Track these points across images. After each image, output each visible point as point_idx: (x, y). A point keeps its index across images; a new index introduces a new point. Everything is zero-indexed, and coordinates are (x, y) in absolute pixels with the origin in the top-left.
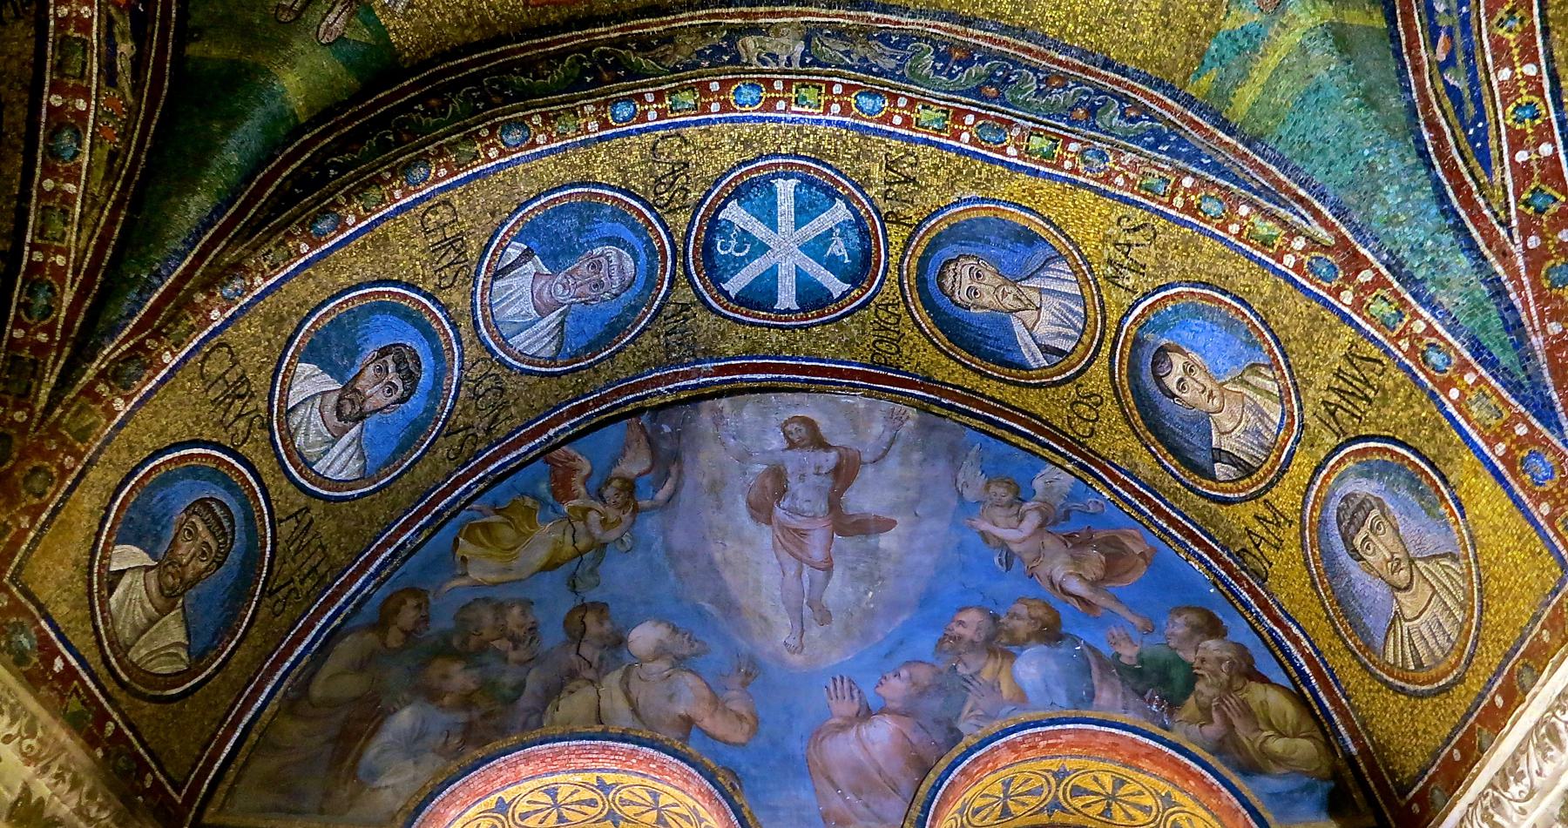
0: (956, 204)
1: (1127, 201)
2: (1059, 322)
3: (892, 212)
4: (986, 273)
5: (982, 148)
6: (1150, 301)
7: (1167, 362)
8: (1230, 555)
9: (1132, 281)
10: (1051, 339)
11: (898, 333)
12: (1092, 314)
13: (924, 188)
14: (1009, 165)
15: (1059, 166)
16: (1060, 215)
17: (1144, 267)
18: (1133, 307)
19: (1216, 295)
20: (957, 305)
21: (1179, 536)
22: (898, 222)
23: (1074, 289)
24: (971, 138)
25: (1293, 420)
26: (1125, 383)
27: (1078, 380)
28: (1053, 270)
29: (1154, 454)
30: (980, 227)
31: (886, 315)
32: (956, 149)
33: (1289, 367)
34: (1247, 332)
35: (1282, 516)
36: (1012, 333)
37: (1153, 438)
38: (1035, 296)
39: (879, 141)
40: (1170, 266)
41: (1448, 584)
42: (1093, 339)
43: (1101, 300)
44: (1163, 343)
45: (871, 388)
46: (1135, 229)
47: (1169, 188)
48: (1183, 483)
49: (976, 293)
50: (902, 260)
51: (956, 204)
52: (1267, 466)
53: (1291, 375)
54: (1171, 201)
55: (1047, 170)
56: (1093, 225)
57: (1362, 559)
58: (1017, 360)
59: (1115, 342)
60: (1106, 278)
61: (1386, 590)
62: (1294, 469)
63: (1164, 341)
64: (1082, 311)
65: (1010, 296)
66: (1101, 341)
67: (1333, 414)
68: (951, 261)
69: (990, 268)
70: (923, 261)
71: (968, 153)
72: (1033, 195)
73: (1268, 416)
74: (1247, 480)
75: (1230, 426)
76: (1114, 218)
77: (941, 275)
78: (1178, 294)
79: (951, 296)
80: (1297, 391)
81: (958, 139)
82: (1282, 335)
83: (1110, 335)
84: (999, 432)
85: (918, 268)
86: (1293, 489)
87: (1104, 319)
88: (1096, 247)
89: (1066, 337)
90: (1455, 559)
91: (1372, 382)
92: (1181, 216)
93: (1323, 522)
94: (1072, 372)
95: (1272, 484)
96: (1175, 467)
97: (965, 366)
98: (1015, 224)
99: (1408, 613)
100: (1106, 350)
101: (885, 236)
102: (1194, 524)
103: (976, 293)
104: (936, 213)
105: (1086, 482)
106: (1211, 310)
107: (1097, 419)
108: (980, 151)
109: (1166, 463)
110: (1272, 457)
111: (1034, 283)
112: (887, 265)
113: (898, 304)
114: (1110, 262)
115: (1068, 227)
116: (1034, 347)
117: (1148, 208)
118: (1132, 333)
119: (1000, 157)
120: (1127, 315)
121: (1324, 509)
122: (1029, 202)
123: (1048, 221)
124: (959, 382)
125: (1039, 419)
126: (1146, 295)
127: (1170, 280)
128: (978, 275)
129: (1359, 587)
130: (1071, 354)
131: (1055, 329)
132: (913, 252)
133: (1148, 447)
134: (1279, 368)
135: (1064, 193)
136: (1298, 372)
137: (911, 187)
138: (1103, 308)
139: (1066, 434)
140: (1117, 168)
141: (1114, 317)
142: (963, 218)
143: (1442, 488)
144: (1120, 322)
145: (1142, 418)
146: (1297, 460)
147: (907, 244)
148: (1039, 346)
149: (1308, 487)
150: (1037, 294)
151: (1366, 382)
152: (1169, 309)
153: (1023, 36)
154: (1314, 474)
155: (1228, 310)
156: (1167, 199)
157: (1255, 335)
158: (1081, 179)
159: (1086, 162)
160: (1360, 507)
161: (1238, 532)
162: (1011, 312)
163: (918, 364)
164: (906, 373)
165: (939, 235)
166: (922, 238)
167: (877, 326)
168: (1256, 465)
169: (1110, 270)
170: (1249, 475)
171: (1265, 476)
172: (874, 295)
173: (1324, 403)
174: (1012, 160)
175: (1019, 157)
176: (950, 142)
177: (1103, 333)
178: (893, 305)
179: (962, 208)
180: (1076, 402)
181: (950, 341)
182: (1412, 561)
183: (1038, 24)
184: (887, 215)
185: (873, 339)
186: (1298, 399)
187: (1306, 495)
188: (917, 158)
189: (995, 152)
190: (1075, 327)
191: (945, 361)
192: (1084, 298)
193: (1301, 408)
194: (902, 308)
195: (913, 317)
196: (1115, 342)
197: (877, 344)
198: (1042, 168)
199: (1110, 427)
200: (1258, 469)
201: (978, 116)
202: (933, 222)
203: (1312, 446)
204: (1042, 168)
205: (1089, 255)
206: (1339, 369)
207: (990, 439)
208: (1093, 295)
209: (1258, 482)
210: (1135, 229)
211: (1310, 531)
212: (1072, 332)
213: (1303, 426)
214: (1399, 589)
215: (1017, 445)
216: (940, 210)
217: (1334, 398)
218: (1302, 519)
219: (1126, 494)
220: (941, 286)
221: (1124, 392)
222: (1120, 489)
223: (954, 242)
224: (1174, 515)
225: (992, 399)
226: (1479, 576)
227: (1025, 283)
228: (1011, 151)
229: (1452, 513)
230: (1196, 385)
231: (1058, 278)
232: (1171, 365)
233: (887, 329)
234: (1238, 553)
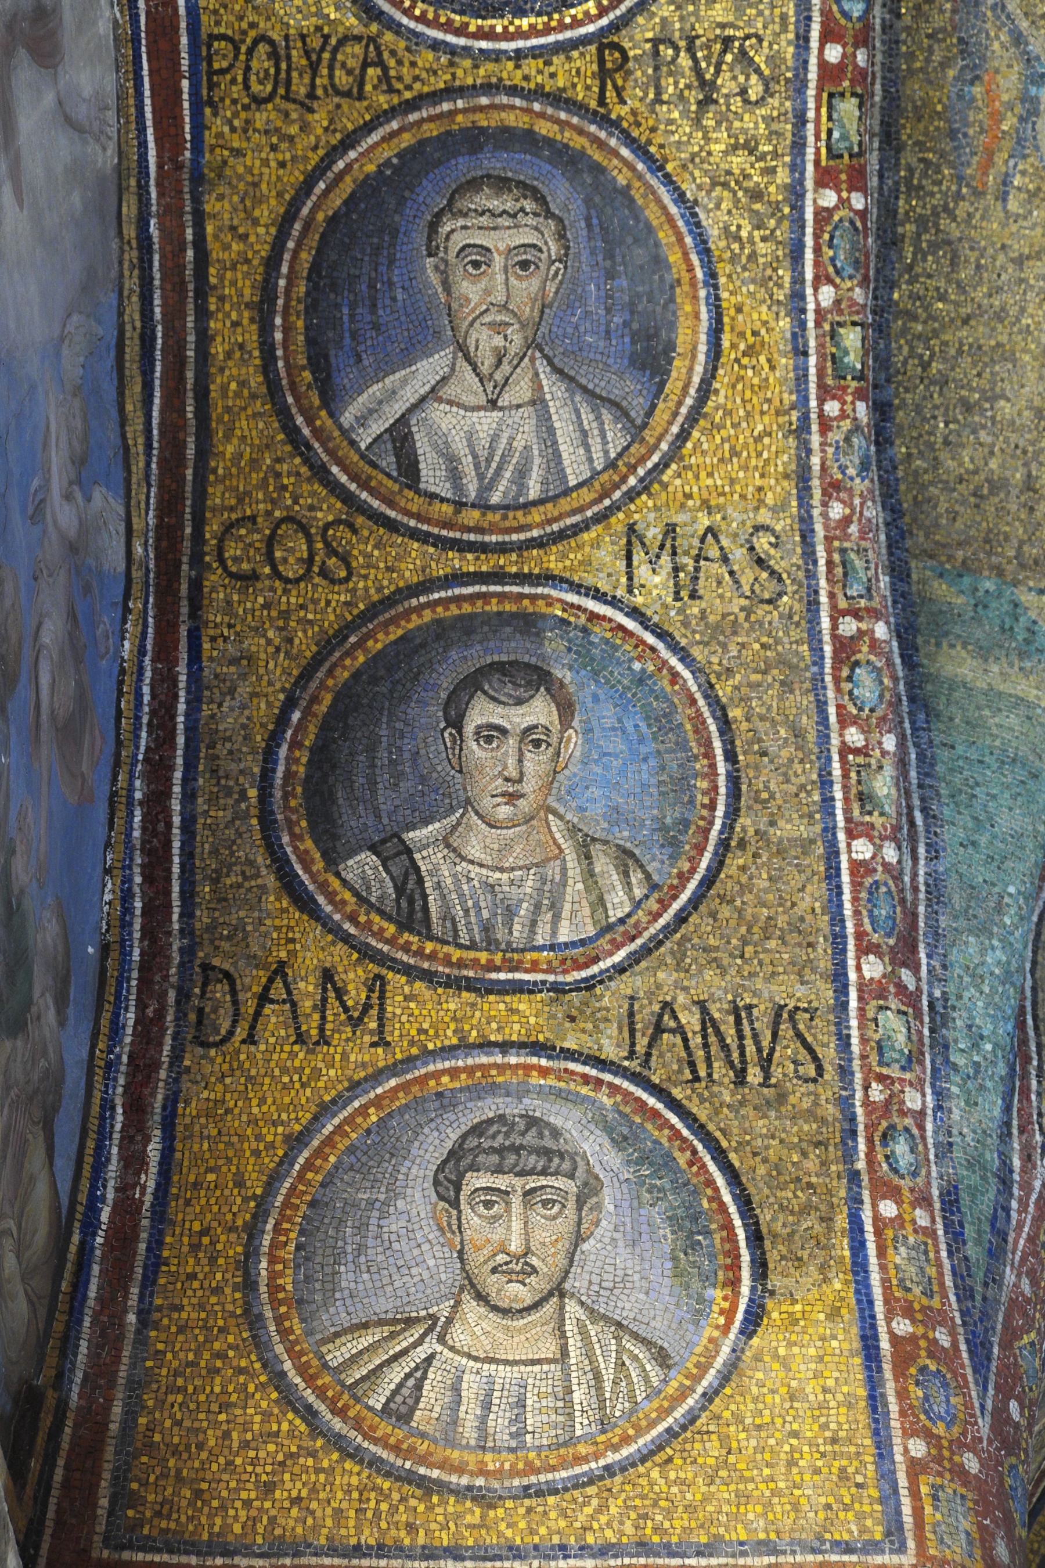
0: (680, 198)
1: (807, 536)
2: (483, 454)
3: (623, 52)
4: (535, 283)
5: (817, 236)
6: (631, 624)
7: (520, 692)
8: (188, 952)
9: (657, 579)
10: (435, 446)
11: (312, 95)
12: (536, 516)
13: (697, 122)
14: (797, 295)
15: (825, 393)
16: (728, 413)
17: (694, 595)
18: (598, 595)
19: (717, 745)
20: (433, 227)
21: (136, 834)
22: (603, 74)
23: (575, 471)
24: (829, 211)
25: (586, 966)
26: (415, 621)
27: (360, 520)
28: (598, 418)
29: (282, 720)
30: (640, 256)
31: (351, 63)
32: (801, 181)
33: (681, 919)
34: (686, 823)
35: (381, 1019)
36: (409, 355)
37: (323, 708)
38: (520, 391)
39: (784, 17)
40: (724, 646)
41: (608, 1376)
42: (479, 530)
43: (577, 530)
44: (558, 673)
45: (136, 40)
46: (760, 562)
47: (863, 603)
48: (264, 797)
49: (476, 264)
50: (514, 91)
51: (680, 198)
52: (456, 954)
53: (669, 930)
54: (844, 613)
55: (812, 371)
56: (732, 482)
57: (455, 1204)
58: (345, 378)
59: (498, 576)
60: (631, 529)
61: (450, 1275)
62: (496, 1005)
63: (561, 673)
64: (534, 492)
65: (498, 341)
66: (483, 548)
67: (659, 1029)
68: (541, 199)
69: (551, 288)
70: (529, 140)
71: (798, 208)
72: (750, 351)
73: (557, 918)
74: (391, 929)
75: (474, 851)
76: (764, 517)
77: (502, 184)
78: (675, 676)
79: (450, 208)
80: (646, 951)
81: (820, 183)
82: (725, 884)
83: (510, 563)
84: (132, 368)
85: (505, 130)
86: (454, 1019)
87: (539, 543)
88: (689, 496)
89: (455, 476)
90: (662, 1358)
91: (777, 1073)
92: (827, 638)
93: (445, 1101)
94: (376, 504)
95: (428, 977)
96: (289, 775)
97: (272, 263)
98: (672, 326)
99: (459, 1336)
100: (469, 563)
101: (563, 48)
102: (188, 854)
103: (476, 264)
104: (641, 150)
105: (127, 596)
106: (682, 745)
107: (287, 581)
108: (809, 230)
109: (283, 752)
110: (483, 957)
111: (553, 388)
112: (497, 56)
113: (391, 90)
114: (671, 530)
115: (709, 433)
116: (397, 409)
117: (811, 575)
118: (541, 606)
119: (809, 275)
120: (577, 588)
121: (477, 1092)
122: (734, 346)
123: (705, 391)
124: (216, 252)
125: (203, 453)
126: (635, 613)
127: (696, 652)
128: (524, 265)
129: (394, 1225)
130: (418, 492)
131: (460, 446)
132: (542, 115)
133: (290, 703)
134: (664, 906)
135: (778, 413)
136: (685, 939)
137: (694, 96)
138: (561, 536)
139: (199, 523)
140: (857, 501)
141: (553, 563)
142: (652, 214)
143: (746, 1274)
144: (553, 578)
145: (356, 675)
146: (523, 1004)
147: (557, 99)
148: (403, 420)
149: (485, 1045)
150: (527, 396)
151: (766, 1064)
152: (637, 666)
153: (884, 244)
154: (522, 1045)
155: (705, 776)
156: (843, 604)
157: (691, 836)
158: (815, 440)
159: (847, 439)
160: (547, 1153)
161: (255, 949)
162: (462, 348)
163: (238, 153)
164: (199, 127)
165: (598, 169)
166: (581, 132)
167: (315, 43)
168: (437, 930)
169: (653, 533)
170: (405, 925)
171: (432, 957)
172: (397, 28)
173: (666, 1005)
174: (810, 299)
175: (818, 311)
176: (810, 168)
177: (503, 549)
178: (385, 77)
179: (673, 210)
180: (304, 528)
181: (333, 221)
182: (559, 1291)
183: (910, 268)
184: (617, 47)
185: (275, 36)
186: (635, 958)
187: (465, 1046)
188: (760, 102)
189: (817, 264)
190: (487, 488)
191: (268, 212)
192: (567, 492)
193: (620, 969)
194: (383, 101)
195: (369, 128)
196: (498, 576)
197: (263, 48)
198: (812, 360)
199: (285, 615)
200: (430, 938)
201: (863, 214)
202: (625, 152)
203: (572, 1019)
204: (812, 360)
205: (665, 486)
206: (749, 1008)
207: (113, 354)
208: (581, 510)
209: (406, 948)
210: (760, 562)
211: (404, 1087)
212: (472, 490)
213: (588, 985)
214: (481, 1297)
215: (123, 422)
216: (657, 166)
217: (691, 1020)
218: (410, 1061)
219: (146, 690)
220: (474, 185)
221: (394, 621)
222: (148, 674)
223: (588, 201)
224: (176, 806)
225: (204, 338)
226: (692, 1418)
227: (542, 366)
228: (827, 295)
229: (729, 1314)
230: (511, 762)
231: (584, 434)
232: (520, 702)
233: (314, 68)
234: (206, 967)
